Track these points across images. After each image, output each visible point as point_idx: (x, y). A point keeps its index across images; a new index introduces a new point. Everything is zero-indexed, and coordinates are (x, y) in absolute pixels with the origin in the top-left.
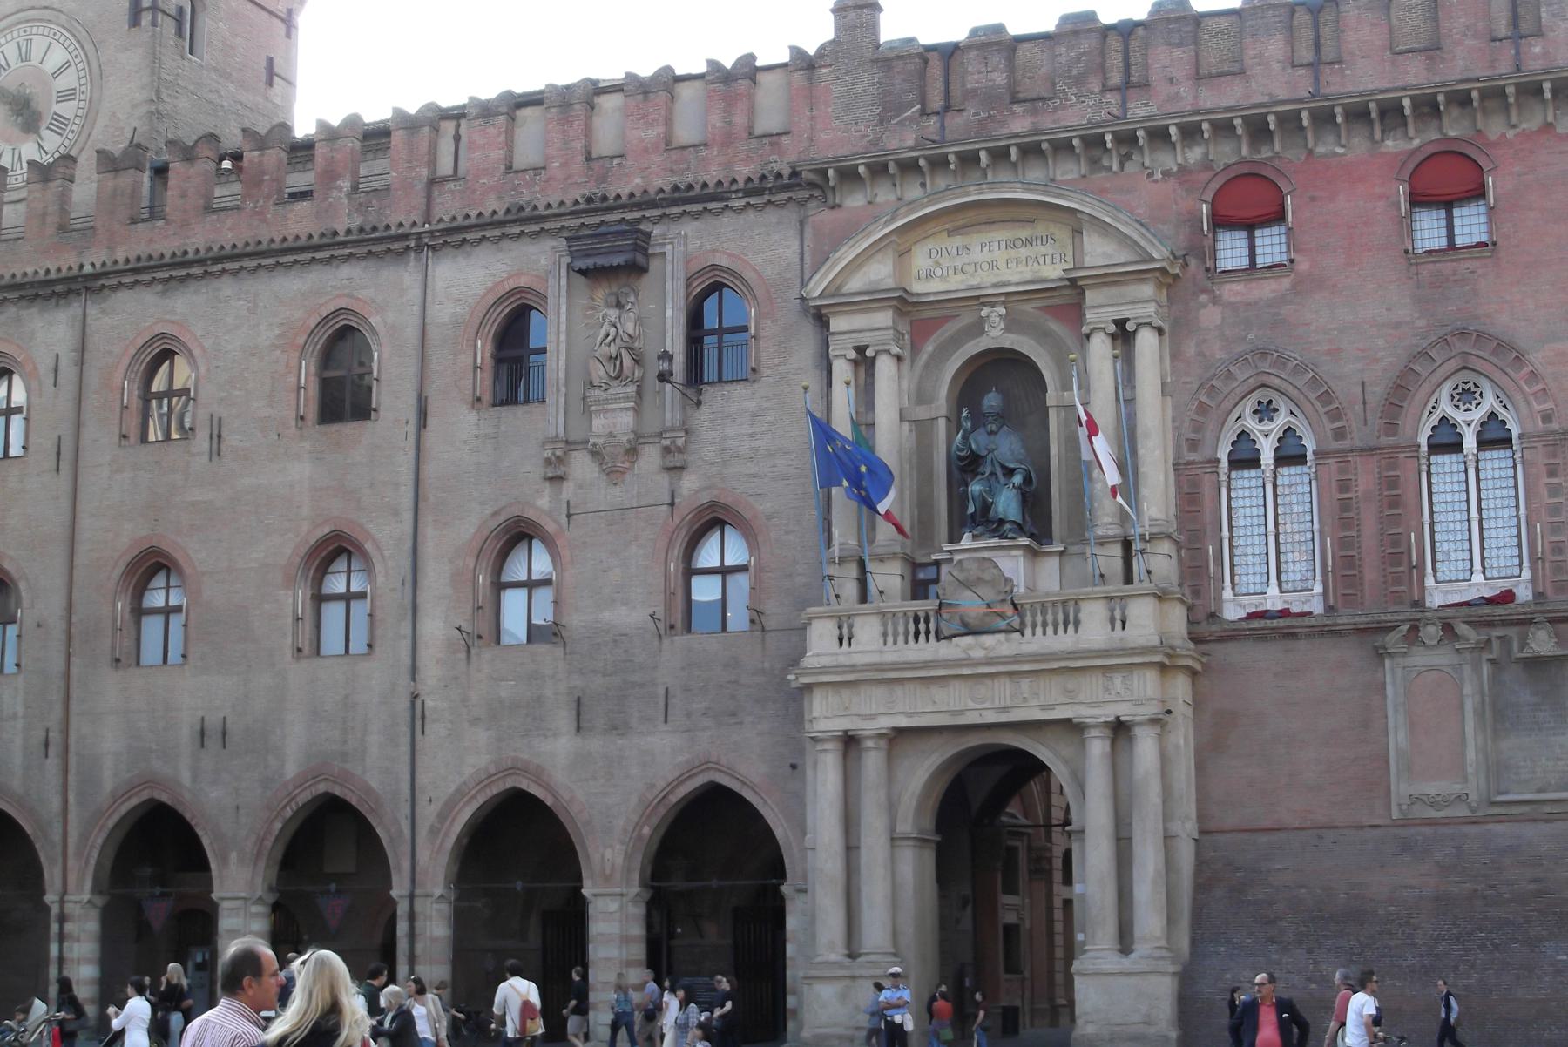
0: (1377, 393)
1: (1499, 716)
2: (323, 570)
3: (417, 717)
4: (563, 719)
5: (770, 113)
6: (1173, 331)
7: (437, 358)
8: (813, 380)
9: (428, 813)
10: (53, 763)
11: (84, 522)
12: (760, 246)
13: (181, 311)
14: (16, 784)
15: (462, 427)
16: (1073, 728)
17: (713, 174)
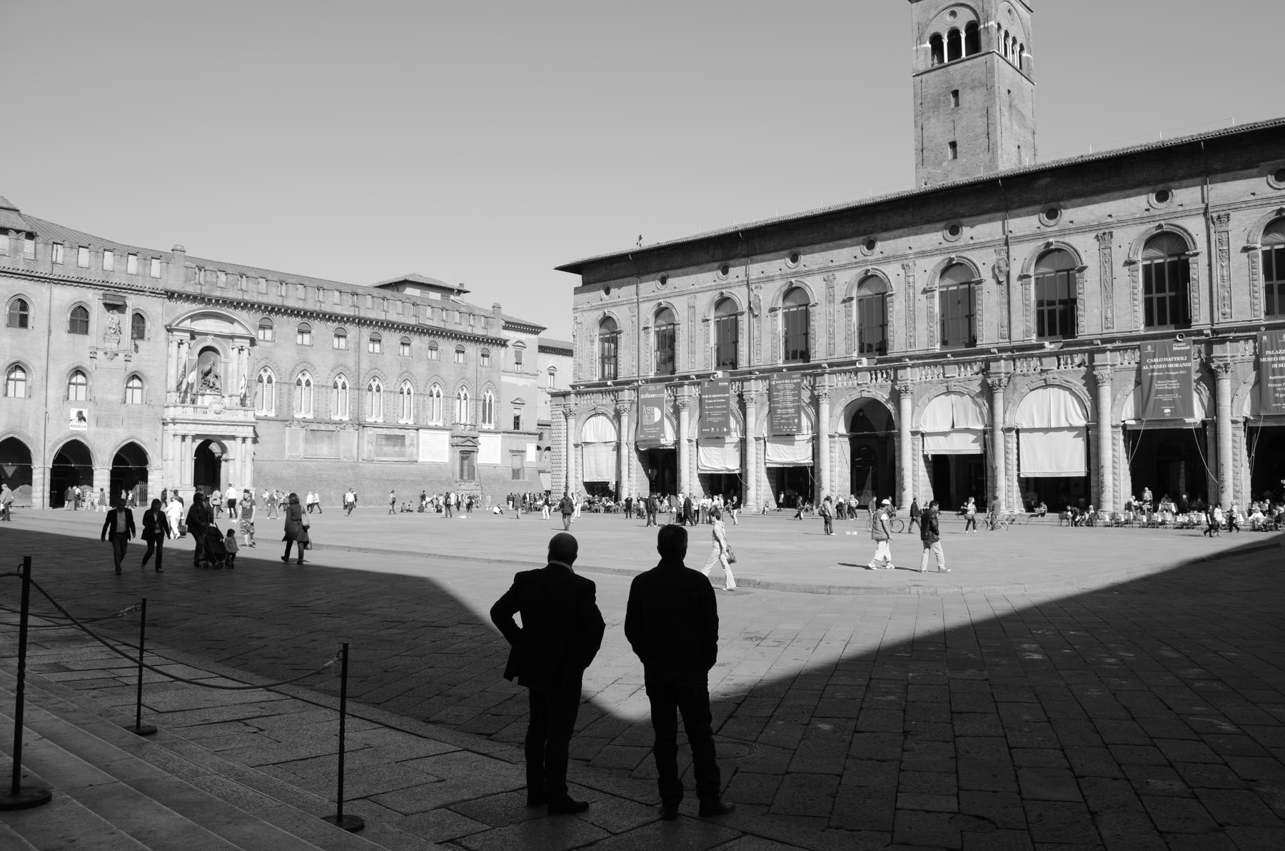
0: (289, 371)
1: (306, 440)
2: (10, 372)
7: (53, 317)
8: (164, 344)
9: (49, 445)
12: (156, 310)
15: (62, 336)
16: (233, 438)
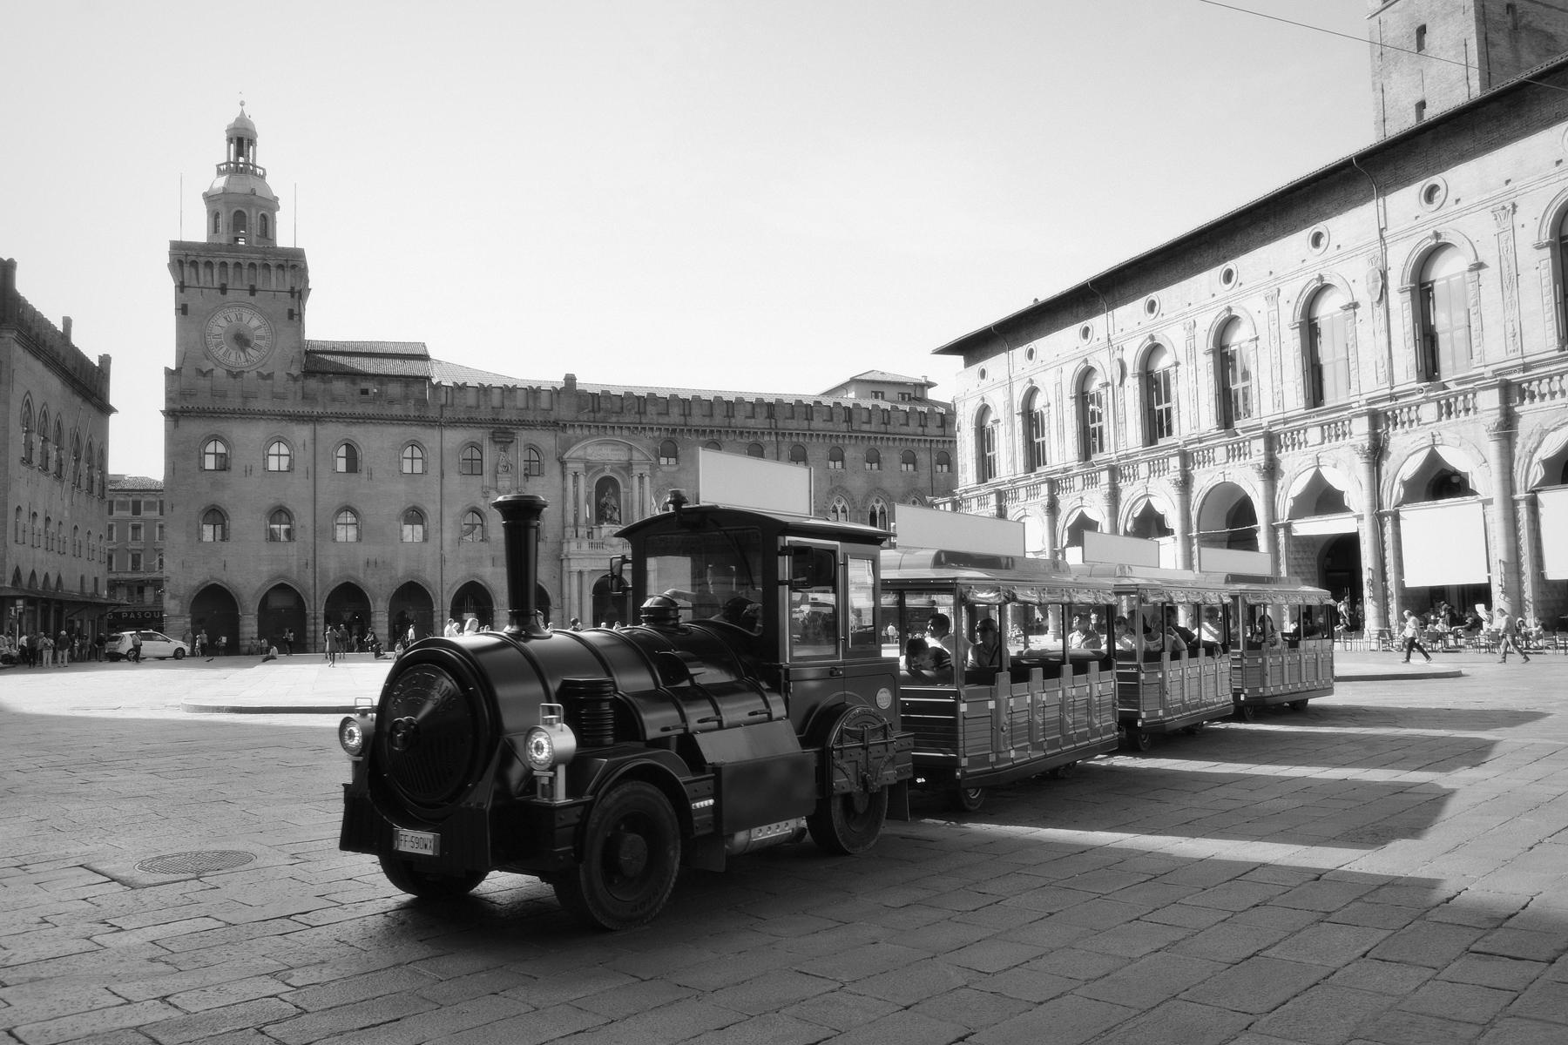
3: (443, 560)
4: (489, 563)
5: (544, 402)
6: (653, 476)
8: (558, 479)
9: (446, 587)
10: (310, 571)
11: (319, 495)
12: (547, 441)
13: (357, 433)
14: (295, 577)
15: (454, 481)
17: (531, 418)
